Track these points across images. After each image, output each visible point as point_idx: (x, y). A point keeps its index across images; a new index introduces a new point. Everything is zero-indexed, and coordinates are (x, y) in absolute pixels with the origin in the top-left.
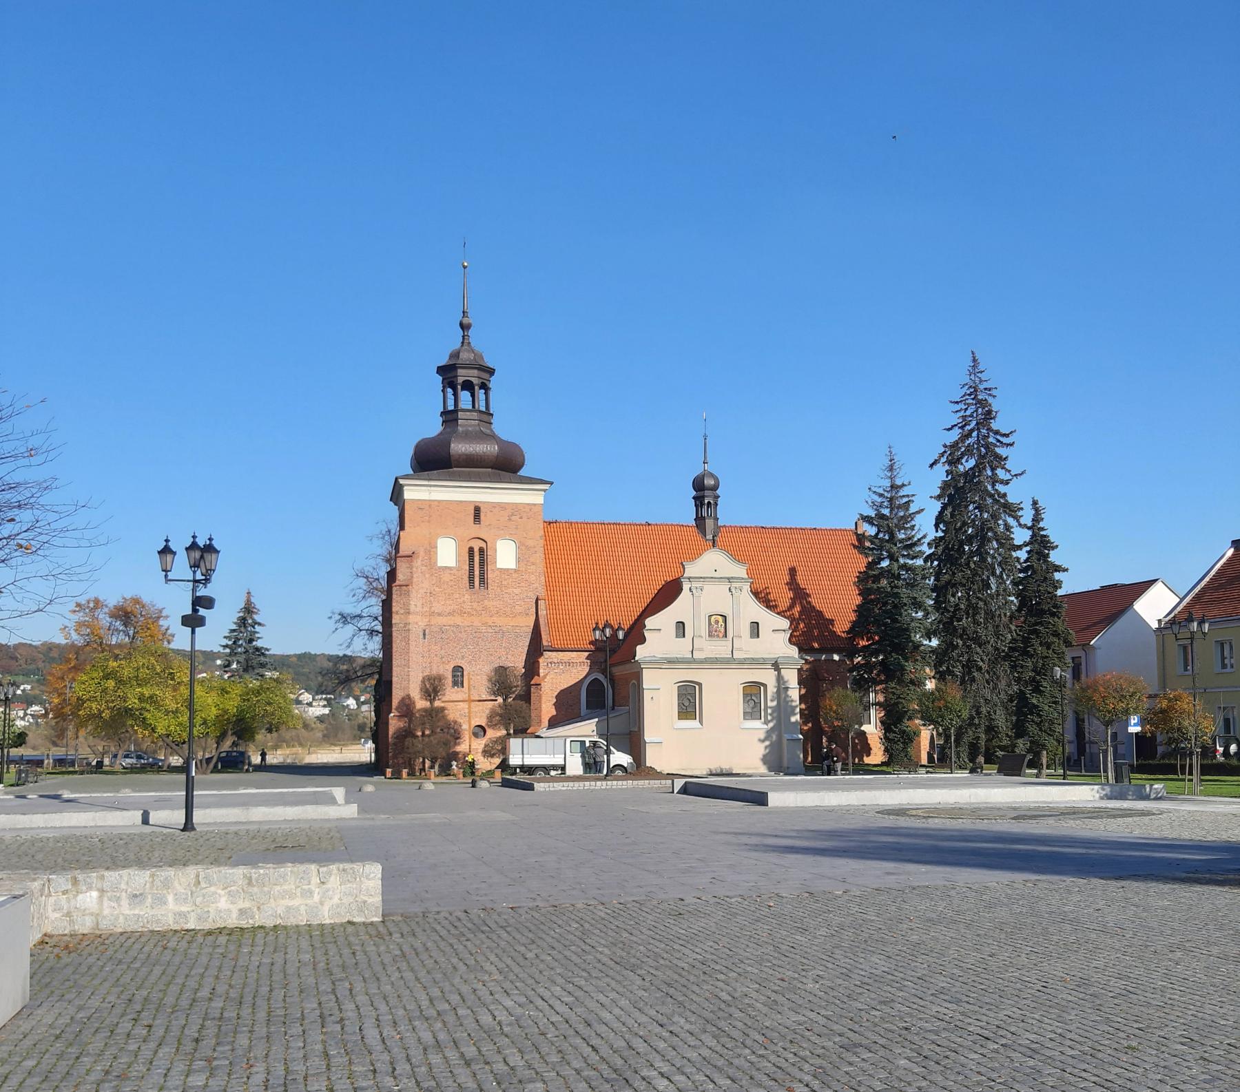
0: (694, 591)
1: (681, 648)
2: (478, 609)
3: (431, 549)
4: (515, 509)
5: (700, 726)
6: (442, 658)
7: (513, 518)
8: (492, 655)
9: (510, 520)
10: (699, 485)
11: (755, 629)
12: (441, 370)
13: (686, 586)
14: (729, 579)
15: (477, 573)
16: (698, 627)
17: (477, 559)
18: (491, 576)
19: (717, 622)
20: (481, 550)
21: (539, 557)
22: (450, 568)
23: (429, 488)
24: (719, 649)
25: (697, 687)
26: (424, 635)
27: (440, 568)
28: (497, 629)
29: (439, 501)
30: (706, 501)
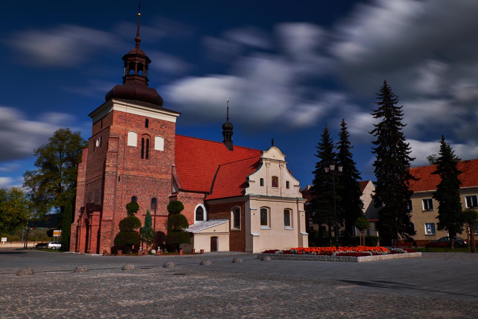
0: (267, 164)
1: (262, 191)
2: (145, 168)
3: (125, 136)
4: (164, 123)
5: (269, 228)
6: (127, 192)
7: (163, 127)
8: (150, 192)
9: (161, 128)
13: (264, 162)
14: (280, 161)
15: (145, 151)
16: (268, 182)
17: (145, 144)
18: (151, 153)
20: (148, 140)
21: (173, 147)
22: (133, 147)
23: (126, 107)
24: (274, 192)
25: (268, 210)
26: (119, 179)
27: (129, 146)
29: (130, 114)
30: (226, 134)
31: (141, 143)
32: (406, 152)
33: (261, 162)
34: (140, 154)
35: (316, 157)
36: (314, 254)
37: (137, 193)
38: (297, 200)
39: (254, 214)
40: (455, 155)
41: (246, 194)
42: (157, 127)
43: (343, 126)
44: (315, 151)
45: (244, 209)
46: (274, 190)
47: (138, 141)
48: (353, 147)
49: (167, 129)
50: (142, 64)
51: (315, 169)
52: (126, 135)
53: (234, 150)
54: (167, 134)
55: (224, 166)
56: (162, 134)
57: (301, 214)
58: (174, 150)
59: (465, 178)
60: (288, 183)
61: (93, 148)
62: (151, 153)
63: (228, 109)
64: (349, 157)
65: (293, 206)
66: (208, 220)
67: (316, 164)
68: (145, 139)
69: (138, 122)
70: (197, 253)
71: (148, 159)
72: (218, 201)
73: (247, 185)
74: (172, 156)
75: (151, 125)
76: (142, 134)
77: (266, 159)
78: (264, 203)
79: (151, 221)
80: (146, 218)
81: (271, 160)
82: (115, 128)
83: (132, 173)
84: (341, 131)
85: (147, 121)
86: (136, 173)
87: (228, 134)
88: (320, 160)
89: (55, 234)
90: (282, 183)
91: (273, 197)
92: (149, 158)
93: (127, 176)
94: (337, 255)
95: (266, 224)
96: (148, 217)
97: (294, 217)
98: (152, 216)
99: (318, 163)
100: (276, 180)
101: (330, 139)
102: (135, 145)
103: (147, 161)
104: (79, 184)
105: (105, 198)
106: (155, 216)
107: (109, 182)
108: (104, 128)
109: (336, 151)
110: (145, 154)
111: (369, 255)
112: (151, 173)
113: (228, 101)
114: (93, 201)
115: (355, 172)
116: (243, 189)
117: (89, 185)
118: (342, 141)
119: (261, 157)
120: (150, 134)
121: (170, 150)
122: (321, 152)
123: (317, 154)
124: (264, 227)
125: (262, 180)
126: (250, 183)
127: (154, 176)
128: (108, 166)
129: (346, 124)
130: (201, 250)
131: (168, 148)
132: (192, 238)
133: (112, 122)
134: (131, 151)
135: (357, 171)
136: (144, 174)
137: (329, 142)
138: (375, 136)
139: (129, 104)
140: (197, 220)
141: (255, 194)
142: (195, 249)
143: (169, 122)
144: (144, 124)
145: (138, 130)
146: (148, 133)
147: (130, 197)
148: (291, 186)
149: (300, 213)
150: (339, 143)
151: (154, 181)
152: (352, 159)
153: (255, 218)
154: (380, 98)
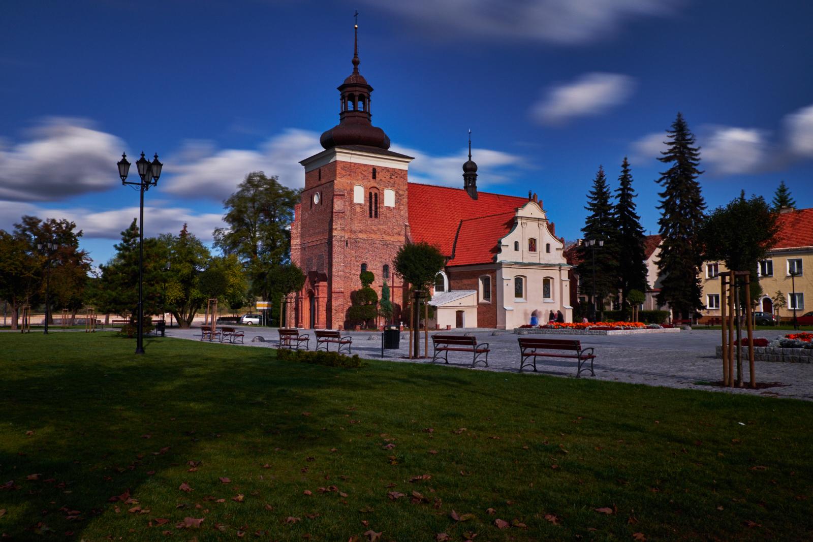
0: (523, 224)
1: (517, 257)
2: (375, 229)
6: (356, 258)
7: (393, 177)
12: (340, 88)
13: (519, 221)
14: (539, 219)
15: (373, 208)
16: (524, 246)
17: (373, 200)
18: (381, 210)
20: (376, 194)
21: (405, 201)
22: (360, 204)
23: (350, 155)
24: (530, 258)
25: (524, 279)
26: (347, 244)
28: (384, 242)
29: (355, 164)
31: (368, 199)
32: (700, 207)
33: (516, 222)
34: (368, 212)
35: (587, 210)
36: (569, 329)
37: (367, 259)
38: (560, 267)
39: (507, 285)
40: (791, 199)
41: (497, 262)
42: (387, 177)
43: (625, 168)
44: (586, 201)
45: (495, 278)
46: (531, 255)
47: (365, 197)
48: (637, 195)
49: (398, 178)
50: (364, 95)
51: (585, 226)
52: (352, 190)
53: (478, 199)
54: (398, 185)
55: (467, 222)
56: (392, 186)
57: (564, 284)
58: (407, 205)
59: (792, 234)
60: (548, 245)
61: (309, 203)
62: (381, 210)
63: (470, 144)
64: (631, 210)
65: (554, 274)
66: (450, 290)
67: (586, 218)
68: (373, 194)
69: (364, 173)
70: (441, 330)
71: (377, 218)
72: (463, 268)
73: (499, 250)
74: (404, 213)
75: (379, 176)
76: (370, 187)
77: (522, 218)
78: (519, 272)
79: (388, 292)
80: (383, 289)
81: (527, 218)
82: (340, 182)
83: (361, 236)
84: (623, 174)
85: (374, 171)
86: (363, 236)
87: (471, 177)
88: (592, 213)
89: (259, 306)
90: (541, 247)
91: (530, 264)
92: (378, 216)
93: (355, 239)
94: (590, 329)
95: (522, 297)
96: (385, 289)
97: (555, 287)
98: (390, 287)
99: (589, 218)
100: (533, 242)
101: (605, 187)
102: (362, 202)
103: (377, 220)
104: (293, 248)
105: (334, 267)
106: (393, 287)
107: (337, 247)
108: (323, 181)
109: (614, 201)
110: (373, 212)
111: (620, 329)
112: (382, 235)
113: (470, 133)
114: (314, 269)
115: (638, 229)
116: (494, 254)
117: (306, 250)
118: (622, 187)
119: (516, 215)
120: (378, 187)
121: (403, 205)
122: (593, 204)
123: (588, 206)
124: (519, 299)
125: (516, 243)
126: (502, 248)
127: (385, 239)
128: (336, 229)
129: (629, 165)
130: (447, 326)
131: (400, 203)
132: (435, 312)
133: (335, 175)
134: (358, 209)
135: (641, 228)
136: (374, 237)
137: (605, 190)
138: (663, 186)
139: (353, 152)
140: (436, 290)
141: (509, 260)
142: (439, 325)
143: (400, 170)
144: (371, 175)
145: (365, 184)
146: (376, 185)
147: (359, 264)
148: (552, 249)
149: (563, 282)
150: (618, 190)
151: (386, 244)
152: (635, 212)
153: (508, 288)
154: (671, 137)
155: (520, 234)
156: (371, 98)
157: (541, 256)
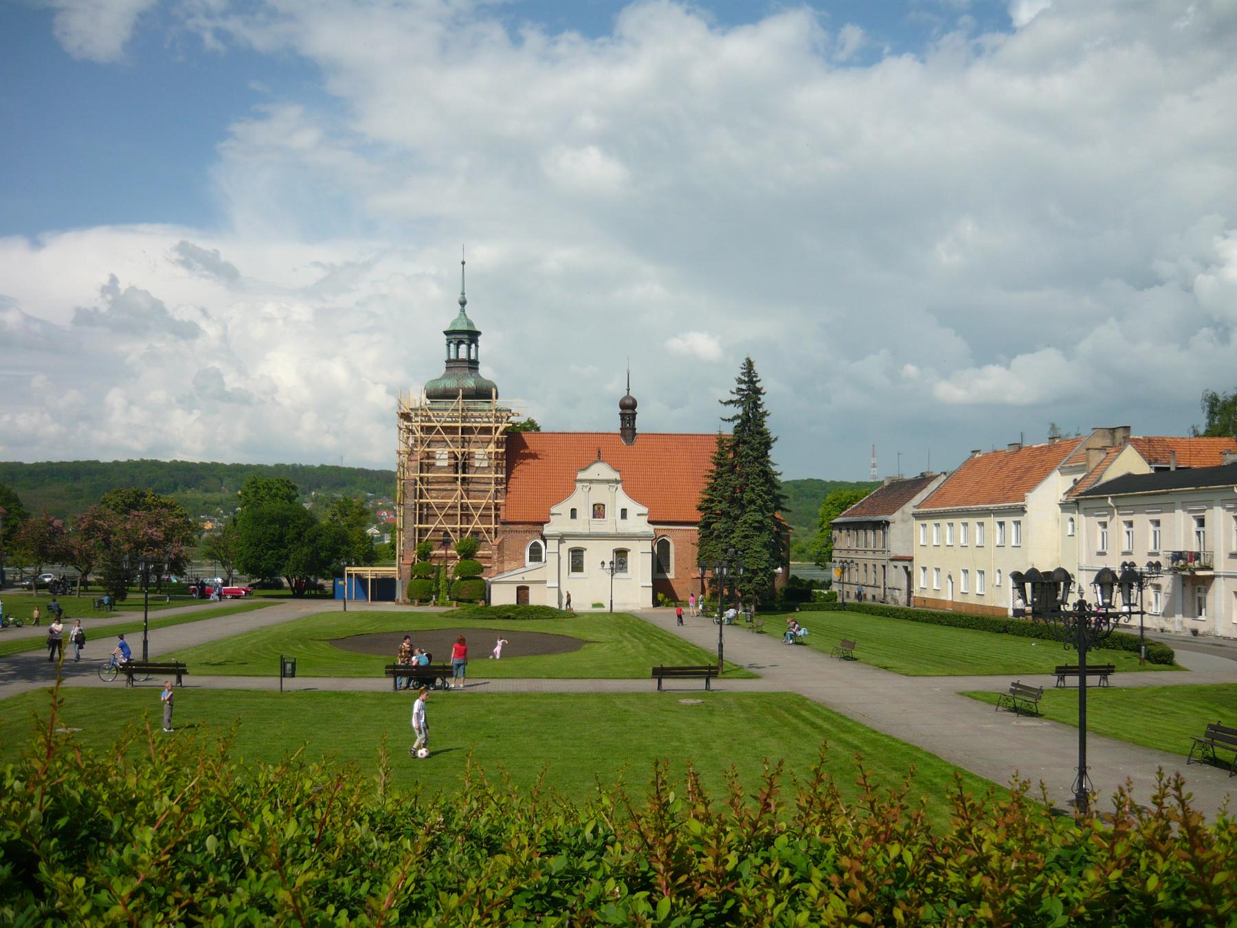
10: (623, 406)
11: (624, 513)
13: (579, 485)
14: (608, 481)
16: (585, 513)
19: (599, 509)
24: (598, 526)
77: (581, 481)
81: (591, 481)
90: (612, 513)
140: (531, 560)
155: (581, 499)
156: (479, 343)
157: (611, 523)
